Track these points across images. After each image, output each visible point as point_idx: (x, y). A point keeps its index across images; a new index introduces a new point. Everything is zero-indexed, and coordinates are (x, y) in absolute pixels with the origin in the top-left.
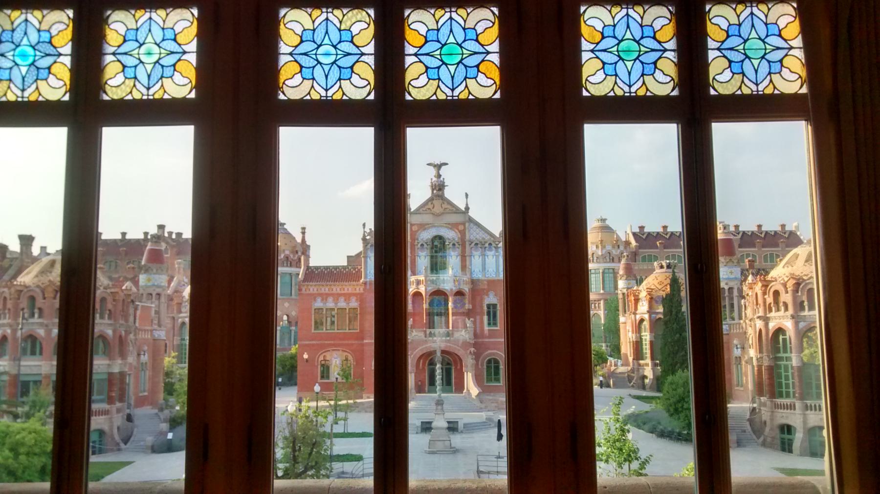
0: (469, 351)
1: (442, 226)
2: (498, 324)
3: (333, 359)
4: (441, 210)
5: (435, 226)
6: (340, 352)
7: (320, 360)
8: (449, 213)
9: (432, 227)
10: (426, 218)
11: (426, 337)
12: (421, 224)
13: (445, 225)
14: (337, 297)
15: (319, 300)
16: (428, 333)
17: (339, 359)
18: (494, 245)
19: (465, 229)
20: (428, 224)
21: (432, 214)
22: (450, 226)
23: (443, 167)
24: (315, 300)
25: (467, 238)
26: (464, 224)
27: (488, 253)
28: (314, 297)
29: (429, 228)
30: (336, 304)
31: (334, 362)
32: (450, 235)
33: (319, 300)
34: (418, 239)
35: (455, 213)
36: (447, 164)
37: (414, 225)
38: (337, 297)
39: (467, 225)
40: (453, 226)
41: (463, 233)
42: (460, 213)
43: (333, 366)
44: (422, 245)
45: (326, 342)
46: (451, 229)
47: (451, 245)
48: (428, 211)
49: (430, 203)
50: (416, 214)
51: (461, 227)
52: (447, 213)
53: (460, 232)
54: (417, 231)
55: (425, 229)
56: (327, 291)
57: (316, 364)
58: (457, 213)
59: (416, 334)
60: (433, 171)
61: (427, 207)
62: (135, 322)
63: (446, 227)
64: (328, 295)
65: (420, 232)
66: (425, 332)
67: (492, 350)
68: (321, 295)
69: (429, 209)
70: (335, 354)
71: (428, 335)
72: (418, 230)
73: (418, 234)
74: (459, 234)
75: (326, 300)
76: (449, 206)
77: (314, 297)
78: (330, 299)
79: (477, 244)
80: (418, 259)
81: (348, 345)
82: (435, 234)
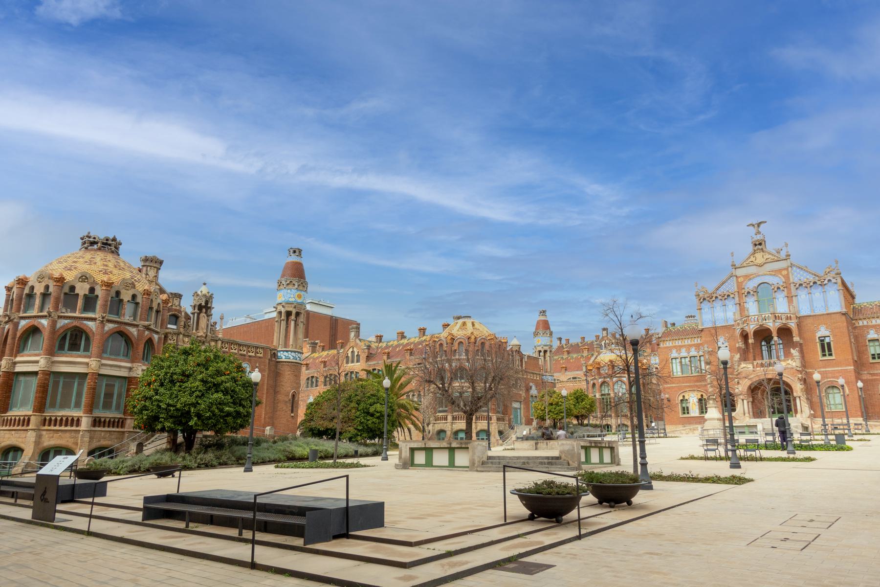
0: (796, 378)
1: (765, 275)
2: (833, 354)
4: (763, 260)
5: (759, 276)
6: (696, 393)
8: (771, 262)
9: (757, 276)
10: (752, 270)
11: (753, 368)
12: (746, 276)
14: (689, 347)
15: (674, 351)
16: (755, 364)
17: (696, 398)
18: (819, 283)
19: (788, 274)
20: (753, 274)
22: (773, 273)
23: (762, 225)
24: (671, 351)
25: (791, 280)
26: (787, 269)
27: (813, 290)
28: (670, 349)
29: (754, 278)
31: (692, 400)
33: (674, 351)
35: (776, 261)
36: (766, 222)
37: (740, 277)
38: (689, 347)
39: (790, 269)
41: (787, 277)
42: (782, 260)
44: (749, 293)
45: (683, 385)
48: (752, 264)
49: (752, 257)
50: (741, 267)
51: (784, 273)
52: (769, 262)
53: (784, 276)
55: (750, 279)
56: (680, 344)
57: (677, 402)
58: (778, 261)
59: (745, 365)
60: (752, 230)
61: (750, 260)
62: (522, 366)
63: (771, 275)
64: (681, 347)
65: (745, 282)
66: (753, 364)
67: (830, 378)
68: (675, 347)
69: (752, 261)
70: (692, 395)
71: (755, 366)
74: (783, 278)
75: (680, 351)
76: (770, 256)
77: (670, 349)
78: (683, 350)
79: (801, 285)
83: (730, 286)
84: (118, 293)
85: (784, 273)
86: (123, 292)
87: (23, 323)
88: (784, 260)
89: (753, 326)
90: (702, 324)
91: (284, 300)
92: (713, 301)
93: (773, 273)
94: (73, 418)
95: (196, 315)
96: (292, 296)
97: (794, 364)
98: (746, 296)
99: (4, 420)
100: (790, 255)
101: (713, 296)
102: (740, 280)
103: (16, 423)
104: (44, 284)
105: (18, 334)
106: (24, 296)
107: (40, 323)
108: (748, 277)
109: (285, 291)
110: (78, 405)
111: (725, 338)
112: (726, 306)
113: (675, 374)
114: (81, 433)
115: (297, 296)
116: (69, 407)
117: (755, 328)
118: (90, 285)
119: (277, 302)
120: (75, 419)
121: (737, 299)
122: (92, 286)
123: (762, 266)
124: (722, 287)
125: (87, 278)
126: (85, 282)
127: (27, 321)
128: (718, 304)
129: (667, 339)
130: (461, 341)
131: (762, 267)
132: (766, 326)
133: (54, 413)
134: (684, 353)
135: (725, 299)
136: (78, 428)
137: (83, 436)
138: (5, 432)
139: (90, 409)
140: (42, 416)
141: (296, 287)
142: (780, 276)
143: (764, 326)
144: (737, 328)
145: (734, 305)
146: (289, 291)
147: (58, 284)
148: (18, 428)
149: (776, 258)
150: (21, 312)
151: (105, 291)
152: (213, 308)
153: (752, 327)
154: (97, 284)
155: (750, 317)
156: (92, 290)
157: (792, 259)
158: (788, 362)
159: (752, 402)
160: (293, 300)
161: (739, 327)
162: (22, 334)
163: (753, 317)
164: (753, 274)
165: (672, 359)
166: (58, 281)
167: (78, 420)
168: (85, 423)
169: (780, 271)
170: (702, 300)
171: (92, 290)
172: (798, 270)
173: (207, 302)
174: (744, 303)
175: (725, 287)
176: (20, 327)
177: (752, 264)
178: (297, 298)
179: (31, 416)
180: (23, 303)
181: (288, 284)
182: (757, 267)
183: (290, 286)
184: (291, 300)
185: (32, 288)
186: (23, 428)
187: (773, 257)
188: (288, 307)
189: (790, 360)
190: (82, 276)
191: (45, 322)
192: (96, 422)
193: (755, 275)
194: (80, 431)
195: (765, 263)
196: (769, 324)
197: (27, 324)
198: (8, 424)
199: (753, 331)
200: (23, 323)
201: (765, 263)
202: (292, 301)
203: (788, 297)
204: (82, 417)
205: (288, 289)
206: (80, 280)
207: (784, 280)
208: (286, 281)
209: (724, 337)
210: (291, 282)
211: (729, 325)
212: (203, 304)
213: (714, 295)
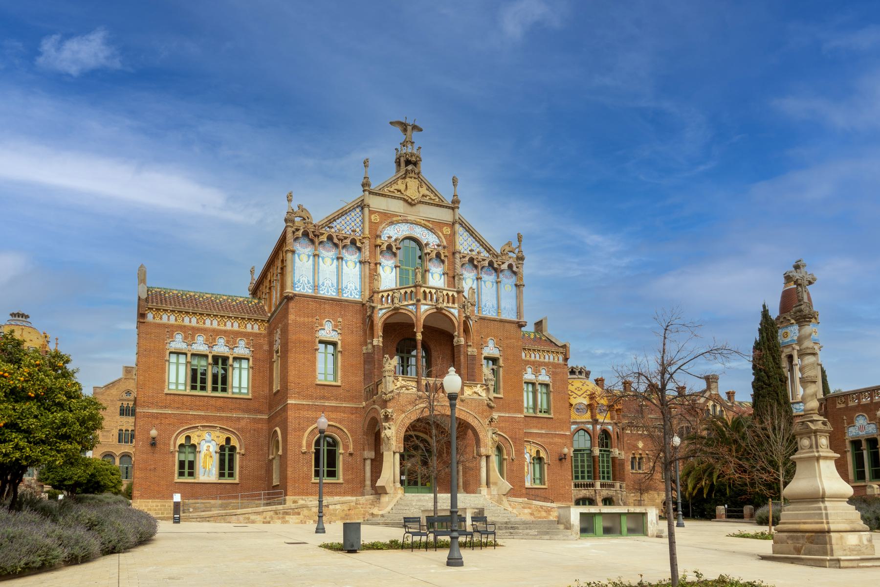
1: (417, 224)
3: (203, 443)
5: (406, 222)
7: (179, 442)
8: (429, 204)
13: (423, 222)
19: (454, 233)
20: (397, 216)
21: (406, 201)
29: (398, 222)
30: (211, 346)
32: (430, 239)
34: (380, 237)
37: (375, 212)
39: (457, 226)
40: (433, 226)
42: (446, 207)
43: (202, 455)
46: (431, 230)
47: (433, 255)
50: (379, 195)
52: (426, 203)
53: (445, 236)
54: (377, 224)
55: (392, 223)
58: (441, 206)
63: (425, 227)
65: (384, 225)
72: (381, 223)
73: (381, 227)
74: (444, 240)
76: (427, 193)
80: (380, 269)
81: (228, 418)
82: (407, 233)
83: (353, 224)
85: (447, 230)
88: (449, 208)
89: (426, 307)
90: (293, 287)
92: (321, 243)
93: (431, 226)
97: (484, 394)
98: (381, 252)
100: (458, 202)
101: (322, 234)
102: (373, 217)
108: (390, 218)
111: (336, 326)
112: (344, 262)
113: (172, 387)
117: (428, 313)
121: (366, 252)
123: (414, 205)
124: (338, 221)
128: (328, 254)
129: (164, 306)
131: (414, 207)
132: (447, 313)
134: (200, 346)
135: (344, 247)
142: (441, 234)
143: (444, 311)
144: (379, 307)
145: (358, 264)
149: (437, 200)
153: (423, 308)
155: (422, 289)
157: (462, 212)
158: (475, 389)
159: (372, 460)
161: (386, 306)
163: (385, 294)
164: (397, 216)
165: (171, 353)
169: (440, 224)
170: (300, 233)
172: (466, 234)
174: (376, 264)
175: (343, 222)
177: (398, 194)
182: (406, 204)
187: (434, 198)
189: (479, 386)
193: (400, 218)
195: (420, 201)
196: (452, 310)
199: (423, 317)
201: (420, 202)
203: (447, 274)
207: (445, 243)
209: (333, 323)
211: (346, 301)
213: (326, 231)
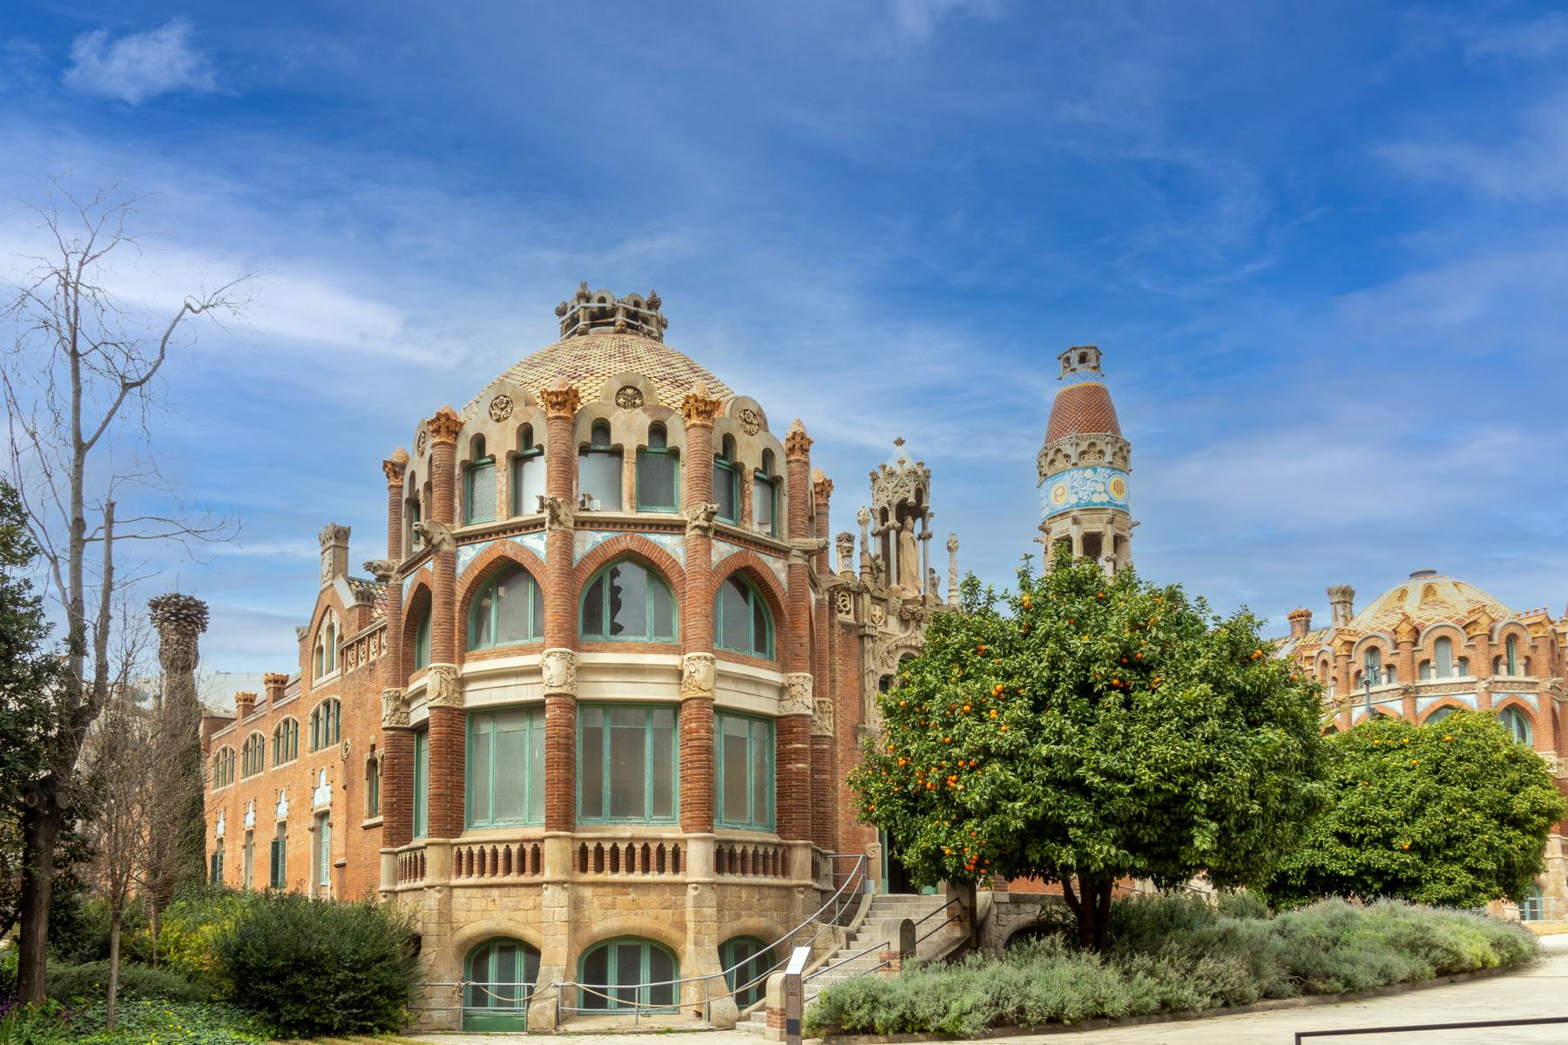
84: (728, 441)
86: (741, 438)
87: (468, 555)
91: (1074, 500)
94: (661, 845)
95: (893, 534)
96: (1100, 488)
99: (460, 855)
103: (501, 863)
104: (513, 424)
105: (460, 592)
106: (457, 471)
107: (522, 547)
109: (1077, 474)
110: (662, 804)
114: (691, 892)
115: (1112, 487)
116: (639, 812)
118: (651, 416)
119: (1046, 513)
120: (669, 848)
122: (655, 418)
125: (639, 393)
126: (634, 405)
127: (478, 546)
130: (1372, 644)
133: (609, 830)
136: (679, 878)
137: (699, 904)
138: (469, 892)
139: (705, 814)
140: (573, 839)
141: (1108, 458)
146: (1089, 473)
147: (562, 414)
148: (508, 879)
150: (457, 523)
151: (699, 432)
152: (932, 515)
154: (670, 411)
156: (658, 431)
160: (1104, 498)
162: (471, 590)
166: (562, 405)
167: (676, 853)
168: (698, 858)
171: (658, 431)
173: (919, 494)
176: (460, 570)
178: (1114, 494)
179: (542, 840)
180: (457, 492)
181: (1083, 453)
183: (1091, 459)
184: (1097, 499)
185: (479, 443)
186: (523, 879)
188: (1091, 521)
190: (624, 388)
191: (536, 544)
192: (725, 859)
194: (686, 884)
197: (481, 557)
198: (476, 867)
200: (468, 555)
202: (1103, 504)
204: (685, 841)
205: (1086, 468)
206: (621, 401)
208: (1077, 445)
210: (1093, 445)
212: (912, 499)
